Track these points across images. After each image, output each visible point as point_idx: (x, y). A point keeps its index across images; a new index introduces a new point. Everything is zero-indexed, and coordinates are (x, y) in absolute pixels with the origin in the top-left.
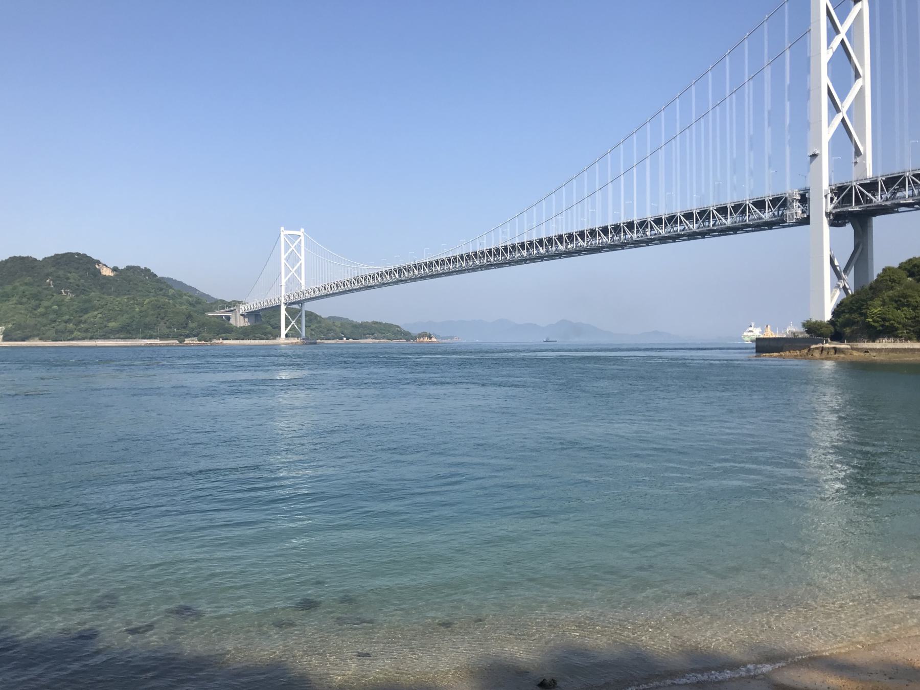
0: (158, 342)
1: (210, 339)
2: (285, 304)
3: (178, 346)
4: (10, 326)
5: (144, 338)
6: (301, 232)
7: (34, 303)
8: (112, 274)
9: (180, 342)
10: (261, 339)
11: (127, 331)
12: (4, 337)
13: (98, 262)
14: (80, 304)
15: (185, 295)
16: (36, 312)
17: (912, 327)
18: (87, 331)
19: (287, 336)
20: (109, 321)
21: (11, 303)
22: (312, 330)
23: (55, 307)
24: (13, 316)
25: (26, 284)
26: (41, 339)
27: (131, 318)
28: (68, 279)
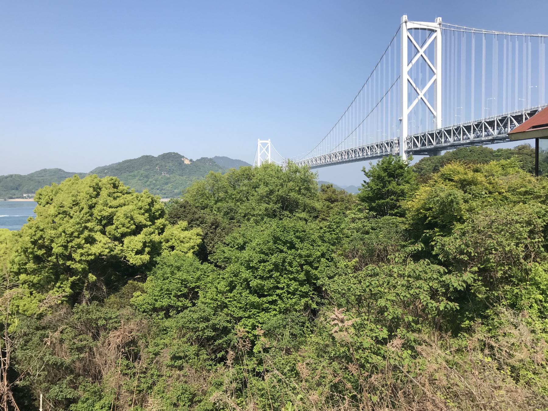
6: (269, 141)
7: (146, 179)
8: (189, 163)
13: (183, 157)
16: (146, 184)
18: (165, 194)
20: (175, 189)
23: (154, 182)
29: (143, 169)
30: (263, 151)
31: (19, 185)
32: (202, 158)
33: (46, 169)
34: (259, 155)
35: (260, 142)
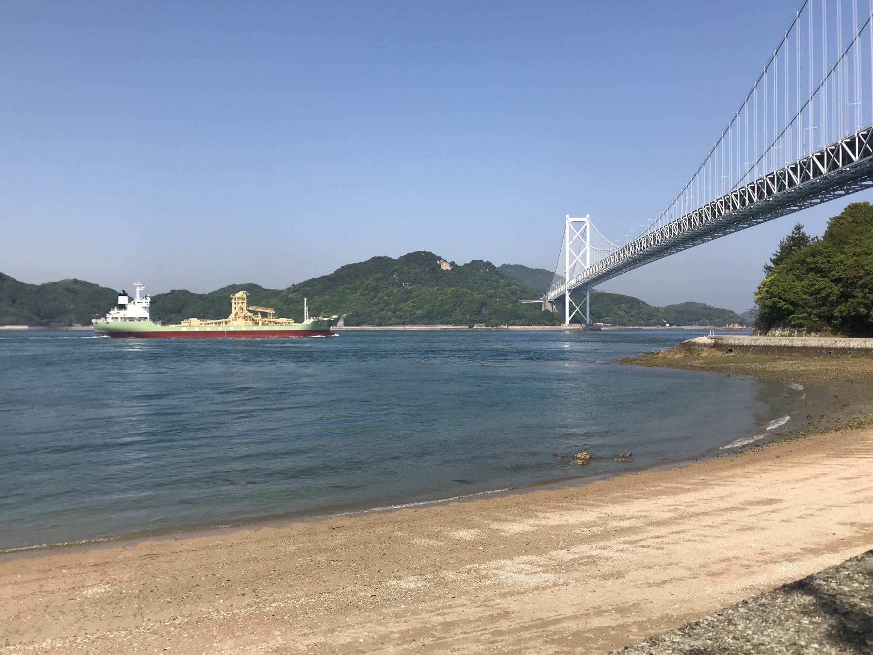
0: (451, 327)
1: (497, 325)
2: (569, 290)
3: (470, 331)
5: (442, 324)
7: (372, 293)
8: (449, 268)
9: (470, 328)
10: (545, 325)
11: (429, 318)
13: (440, 258)
14: (404, 295)
15: (514, 284)
17: (817, 307)
18: (401, 317)
19: (572, 322)
20: (418, 309)
22: (631, 316)
23: (386, 298)
24: (355, 305)
26: (369, 324)
27: (433, 306)
29: (371, 279)
30: (576, 236)
32: (474, 262)
33: (235, 285)
34: (568, 243)
35: (569, 220)
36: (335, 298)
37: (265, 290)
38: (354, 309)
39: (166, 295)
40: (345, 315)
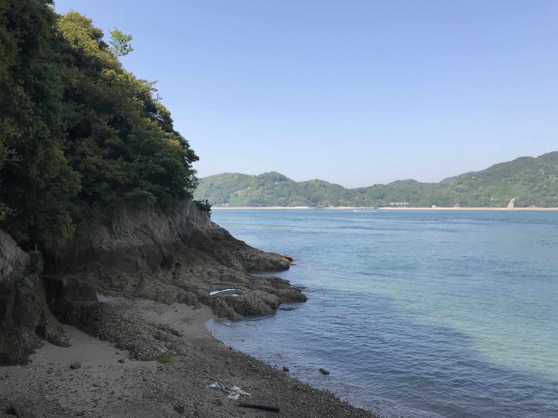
4: (518, 198)
7: (531, 184)
12: (514, 205)
16: (533, 190)
21: (518, 185)
23: (545, 186)
25: (527, 173)
26: (536, 206)
28: (553, 168)
31: (384, 195)
36: (500, 188)
37: (420, 183)
38: (520, 195)
39: (371, 187)
40: (513, 200)
